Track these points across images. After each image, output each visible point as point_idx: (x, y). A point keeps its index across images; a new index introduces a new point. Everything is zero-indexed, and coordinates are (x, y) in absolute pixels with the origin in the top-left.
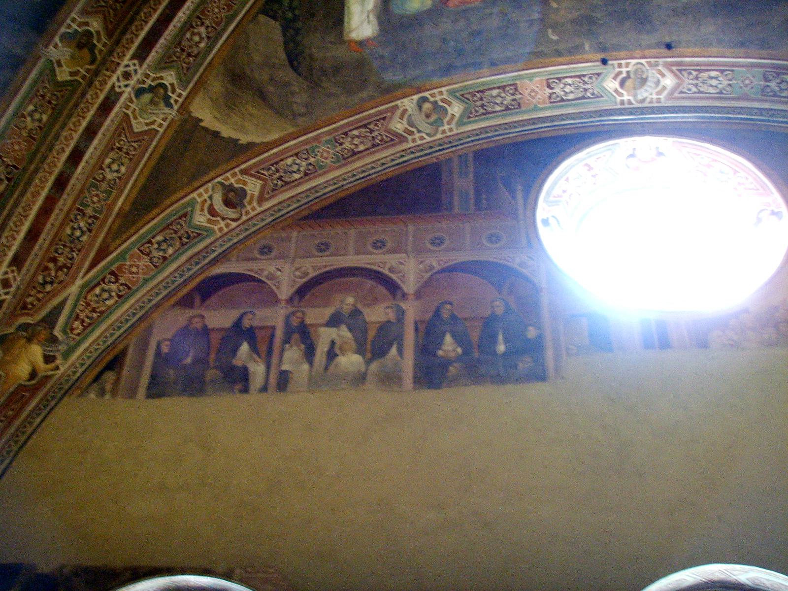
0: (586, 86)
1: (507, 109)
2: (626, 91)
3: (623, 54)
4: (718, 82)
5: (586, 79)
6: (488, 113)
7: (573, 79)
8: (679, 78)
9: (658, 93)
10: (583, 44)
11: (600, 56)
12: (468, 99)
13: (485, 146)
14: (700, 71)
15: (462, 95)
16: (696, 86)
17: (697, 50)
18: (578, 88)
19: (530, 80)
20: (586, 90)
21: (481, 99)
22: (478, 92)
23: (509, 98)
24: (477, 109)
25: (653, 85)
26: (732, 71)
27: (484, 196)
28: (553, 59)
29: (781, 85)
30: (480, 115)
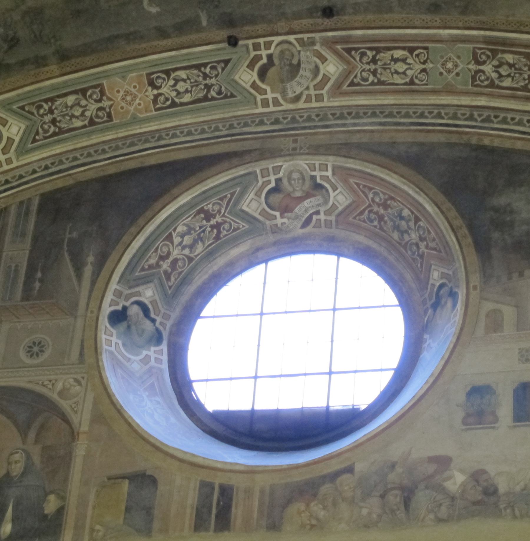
0: (208, 81)
1: (92, 122)
2: (267, 84)
3: (260, 28)
4: (407, 66)
5: (208, 70)
6: (62, 131)
7: (187, 71)
8: (348, 63)
9: (320, 86)
10: (198, 17)
11: (224, 34)
12: (32, 114)
13: (60, 184)
14: (378, 50)
15: (22, 108)
16: (374, 73)
17: (370, 17)
18: (196, 84)
19: (124, 78)
20: (208, 87)
21: (51, 111)
22: (46, 101)
23: (93, 107)
24: (46, 127)
25: (308, 74)
26: (426, 48)
27: (39, 275)
28: (155, 43)
29: (501, 70)
30: (51, 136)
